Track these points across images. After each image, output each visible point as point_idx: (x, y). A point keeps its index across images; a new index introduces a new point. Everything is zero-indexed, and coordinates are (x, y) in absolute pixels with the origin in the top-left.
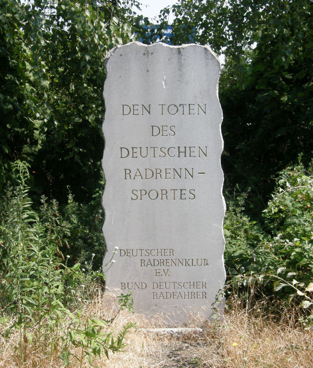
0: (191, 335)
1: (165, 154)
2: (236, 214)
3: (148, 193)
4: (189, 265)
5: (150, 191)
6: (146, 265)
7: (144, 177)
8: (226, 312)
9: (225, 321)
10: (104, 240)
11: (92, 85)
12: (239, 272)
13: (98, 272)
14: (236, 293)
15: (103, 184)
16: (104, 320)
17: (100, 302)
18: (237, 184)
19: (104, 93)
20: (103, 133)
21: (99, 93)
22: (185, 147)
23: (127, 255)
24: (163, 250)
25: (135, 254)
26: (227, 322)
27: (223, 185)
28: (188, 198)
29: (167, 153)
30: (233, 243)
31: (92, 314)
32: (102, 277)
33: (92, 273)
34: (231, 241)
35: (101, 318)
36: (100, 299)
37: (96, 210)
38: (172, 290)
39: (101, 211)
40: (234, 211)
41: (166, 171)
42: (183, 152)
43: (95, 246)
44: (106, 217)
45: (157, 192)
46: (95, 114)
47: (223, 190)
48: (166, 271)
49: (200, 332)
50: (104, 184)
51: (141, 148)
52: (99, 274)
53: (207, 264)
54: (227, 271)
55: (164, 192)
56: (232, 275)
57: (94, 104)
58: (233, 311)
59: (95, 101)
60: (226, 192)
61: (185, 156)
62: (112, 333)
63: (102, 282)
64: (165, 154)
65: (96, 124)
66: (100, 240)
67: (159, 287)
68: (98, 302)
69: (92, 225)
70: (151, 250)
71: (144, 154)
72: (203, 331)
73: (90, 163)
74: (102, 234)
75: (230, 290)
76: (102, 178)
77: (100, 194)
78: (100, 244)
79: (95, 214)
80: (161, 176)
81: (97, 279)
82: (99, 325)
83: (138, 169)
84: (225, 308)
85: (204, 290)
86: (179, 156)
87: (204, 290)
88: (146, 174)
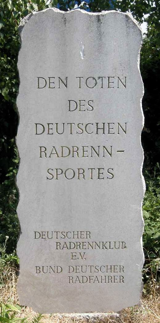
0: (108, 320)
1: (83, 130)
2: (156, 195)
3: (64, 172)
4: (106, 248)
5: (67, 170)
6: (61, 248)
7: (60, 155)
8: (144, 296)
9: (142, 306)
10: (18, 222)
11: (5, 56)
12: (158, 256)
13: (11, 255)
14: (154, 277)
15: (17, 162)
16: (19, 305)
17: (14, 286)
18: (158, 163)
19: (18, 64)
20: (17, 108)
21: (13, 64)
22: (104, 124)
23: (42, 238)
24: (79, 233)
25: (50, 236)
26: (145, 306)
27: (143, 164)
28: (106, 178)
29: (84, 129)
30: (153, 225)
31: (6, 298)
32: (16, 260)
33: (6, 257)
34: (150, 223)
35: (14, 303)
36: (14, 283)
37: (10, 190)
38: (88, 274)
39: (15, 191)
40: (154, 191)
41: (83, 149)
42: (101, 128)
43: (9, 228)
44: (20, 198)
45: (74, 171)
46: (9, 88)
47: (143, 169)
48: (82, 254)
49: (117, 318)
50: (19, 163)
51: (57, 124)
52: (13, 257)
53: (125, 247)
54: (145, 254)
55: (81, 171)
56: (151, 258)
57: (8, 76)
58: (151, 296)
59: (8, 73)
60: (146, 171)
61: (104, 133)
62: (26, 319)
63: (16, 266)
64: (83, 130)
65: (10, 98)
66: (14, 222)
67: (75, 271)
68: (12, 287)
69: (6, 206)
70: (67, 233)
71: (60, 131)
72: (120, 316)
73: (3, 140)
74: (16, 215)
75: (148, 273)
76: (16, 156)
77: (14, 173)
78: (14, 226)
79: (9, 195)
80: (78, 154)
81: (11, 263)
82: (13, 310)
83: (54, 147)
84: (143, 293)
85: (122, 274)
86: (97, 133)
87: (122, 274)
88: (62, 152)
